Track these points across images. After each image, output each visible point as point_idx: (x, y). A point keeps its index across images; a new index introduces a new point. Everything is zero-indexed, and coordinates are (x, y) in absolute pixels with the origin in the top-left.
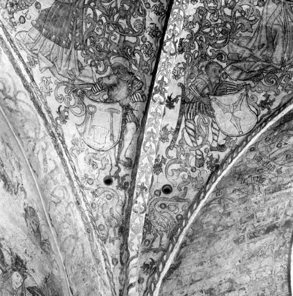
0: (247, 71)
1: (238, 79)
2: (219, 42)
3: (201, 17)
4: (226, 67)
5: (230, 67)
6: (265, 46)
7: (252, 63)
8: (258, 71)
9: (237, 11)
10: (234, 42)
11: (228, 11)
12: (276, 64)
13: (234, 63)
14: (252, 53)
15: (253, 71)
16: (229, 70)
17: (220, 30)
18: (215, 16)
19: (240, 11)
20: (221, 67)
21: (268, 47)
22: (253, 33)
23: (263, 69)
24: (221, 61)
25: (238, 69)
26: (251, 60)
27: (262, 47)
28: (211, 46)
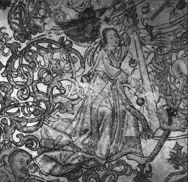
0: (63, 164)
1: (50, 173)
2: (29, 125)
3: (3, 94)
4: (36, 157)
5: (42, 156)
6: (88, 133)
7: (69, 153)
8: (76, 164)
9: (55, 88)
10: (50, 125)
11: (42, 88)
12: (99, 158)
13: (47, 152)
14: (71, 140)
15: (70, 164)
16: (40, 161)
17: (32, 109)
18: (25, 92)
19: (59, 87)
20: (31, 156)
21: (91, 134)
22: (74, 115)
23: (83, 163)
24: (31, 148)
25: (52, 159)
26: (70, 148)
27: (84, 133)
28: (19, 130)
